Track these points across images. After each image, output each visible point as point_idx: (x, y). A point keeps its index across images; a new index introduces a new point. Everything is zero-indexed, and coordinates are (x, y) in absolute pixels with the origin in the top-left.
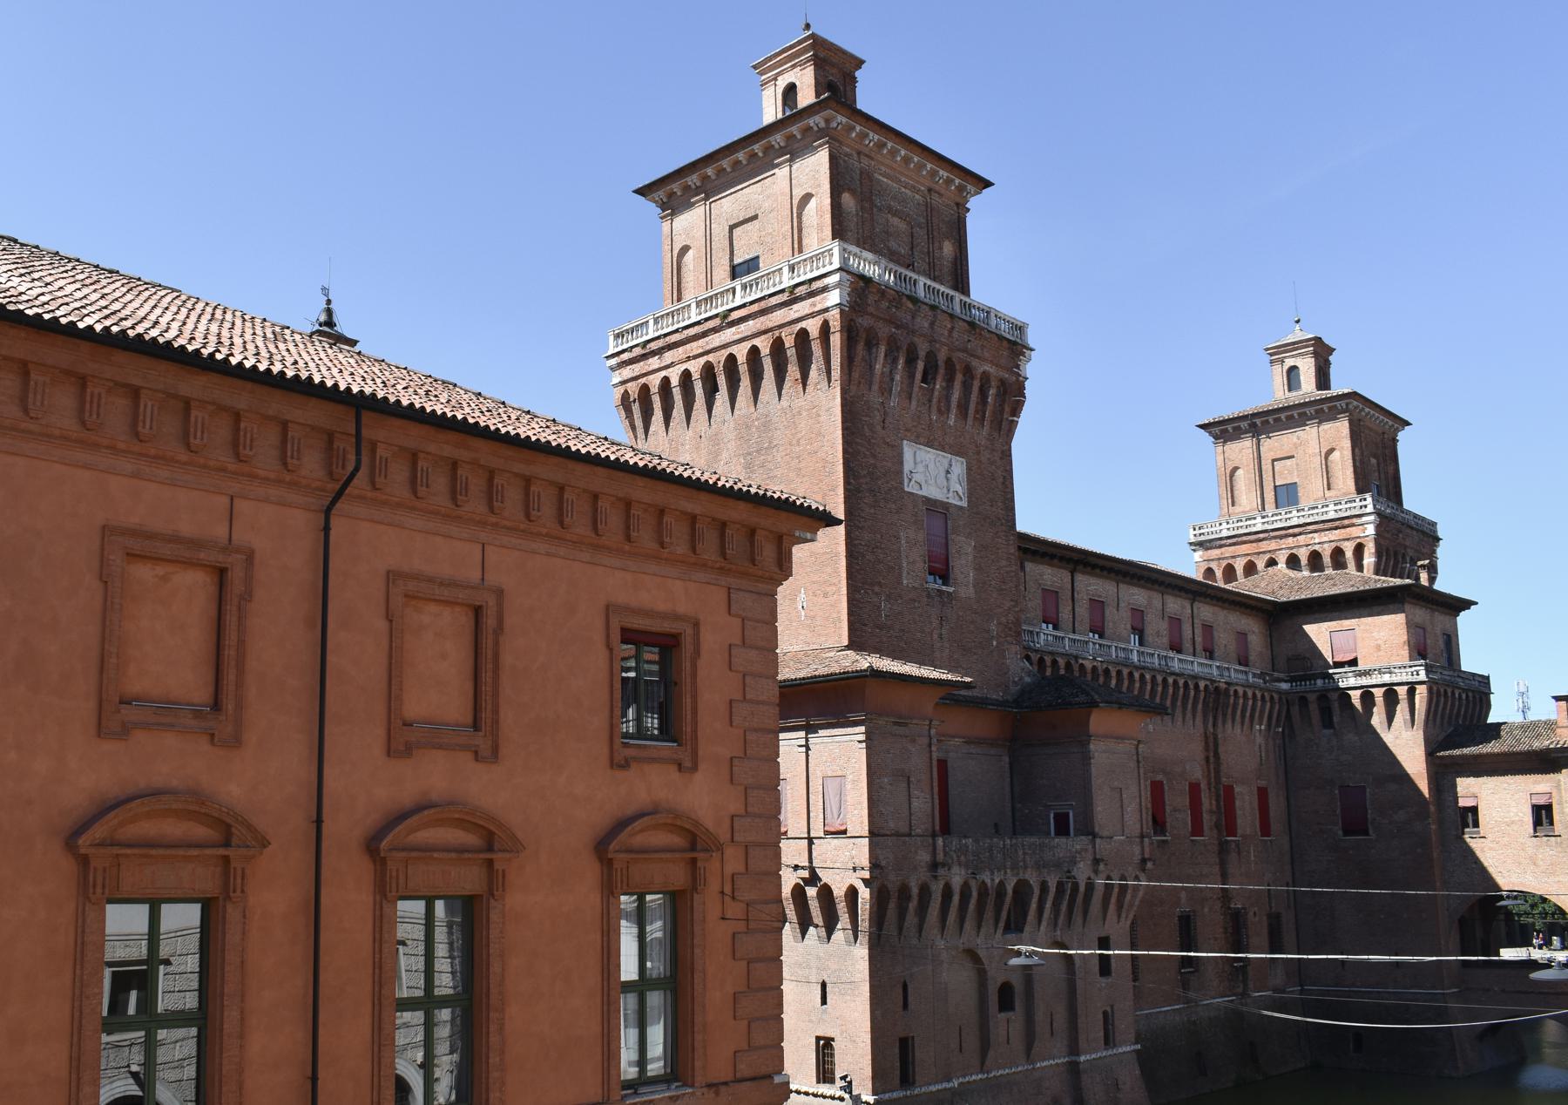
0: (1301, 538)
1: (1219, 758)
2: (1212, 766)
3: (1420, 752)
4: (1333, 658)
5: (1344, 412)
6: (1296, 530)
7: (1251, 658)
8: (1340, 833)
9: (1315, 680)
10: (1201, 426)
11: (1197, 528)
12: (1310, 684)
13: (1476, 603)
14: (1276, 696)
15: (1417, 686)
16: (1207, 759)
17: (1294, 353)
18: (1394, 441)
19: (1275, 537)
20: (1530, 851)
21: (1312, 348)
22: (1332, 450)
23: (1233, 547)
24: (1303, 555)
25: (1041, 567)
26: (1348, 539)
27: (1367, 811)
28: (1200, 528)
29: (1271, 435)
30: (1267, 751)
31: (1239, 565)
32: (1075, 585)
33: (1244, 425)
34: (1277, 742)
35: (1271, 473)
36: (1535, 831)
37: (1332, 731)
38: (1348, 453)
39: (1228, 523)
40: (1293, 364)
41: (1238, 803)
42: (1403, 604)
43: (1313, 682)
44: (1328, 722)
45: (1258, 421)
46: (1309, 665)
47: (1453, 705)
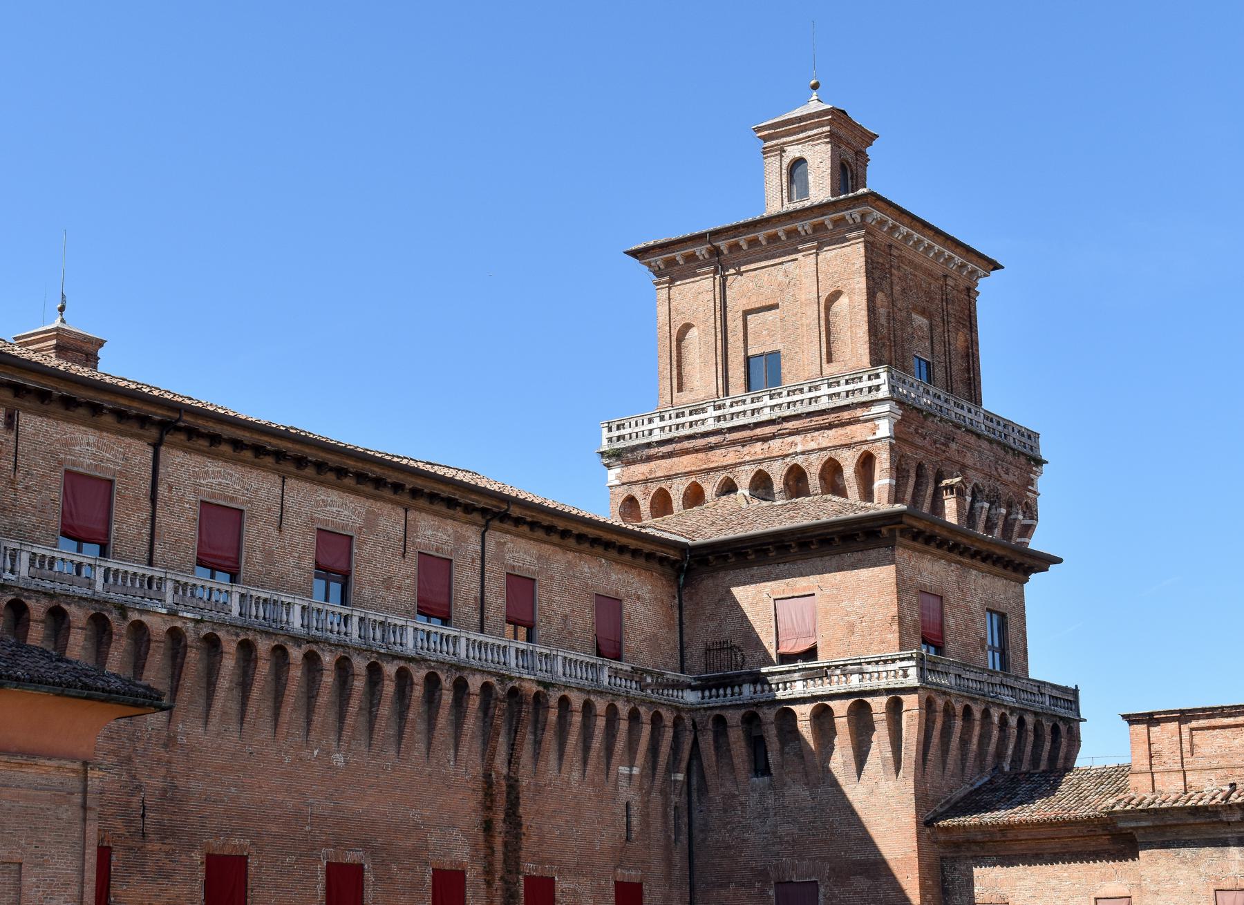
0: (776, 444)
1: (520, 825)
2: (498, 842)
3: (907, 819)
4: (778, 648)
5: (858, 228)
6: (767, 430)
7: (627, 644)
9: (740, 686)
10: (635, 254)
11: (614, 428)
12: (733, 695)
13: (1058, 561)
14: (668, 716)
15: (902, 697)
16: (488, 827)
17: (801, 136)
18: (970, 293)
19: (734, 443)
21: (828, 128)
22: (836, 295)
23: (668, 461)
24: (777, 472)
25: (69, 428)
26: (848, 446)
28: (618, 428)
29: (743, 268)
30: (645, 818)
31: (677, 491)
32: (162, 470)
33: (701, 251)
34: (674, 799)
35: (741, 335)
37: (766, 779)
38: (861, 300)
39: (662, 419)
40: (798, 155)
42: (893, 550)
43: (736, 689)
44: (761, 767)
45: (723, 245)
46: (739, 659)
47: (985, 737)
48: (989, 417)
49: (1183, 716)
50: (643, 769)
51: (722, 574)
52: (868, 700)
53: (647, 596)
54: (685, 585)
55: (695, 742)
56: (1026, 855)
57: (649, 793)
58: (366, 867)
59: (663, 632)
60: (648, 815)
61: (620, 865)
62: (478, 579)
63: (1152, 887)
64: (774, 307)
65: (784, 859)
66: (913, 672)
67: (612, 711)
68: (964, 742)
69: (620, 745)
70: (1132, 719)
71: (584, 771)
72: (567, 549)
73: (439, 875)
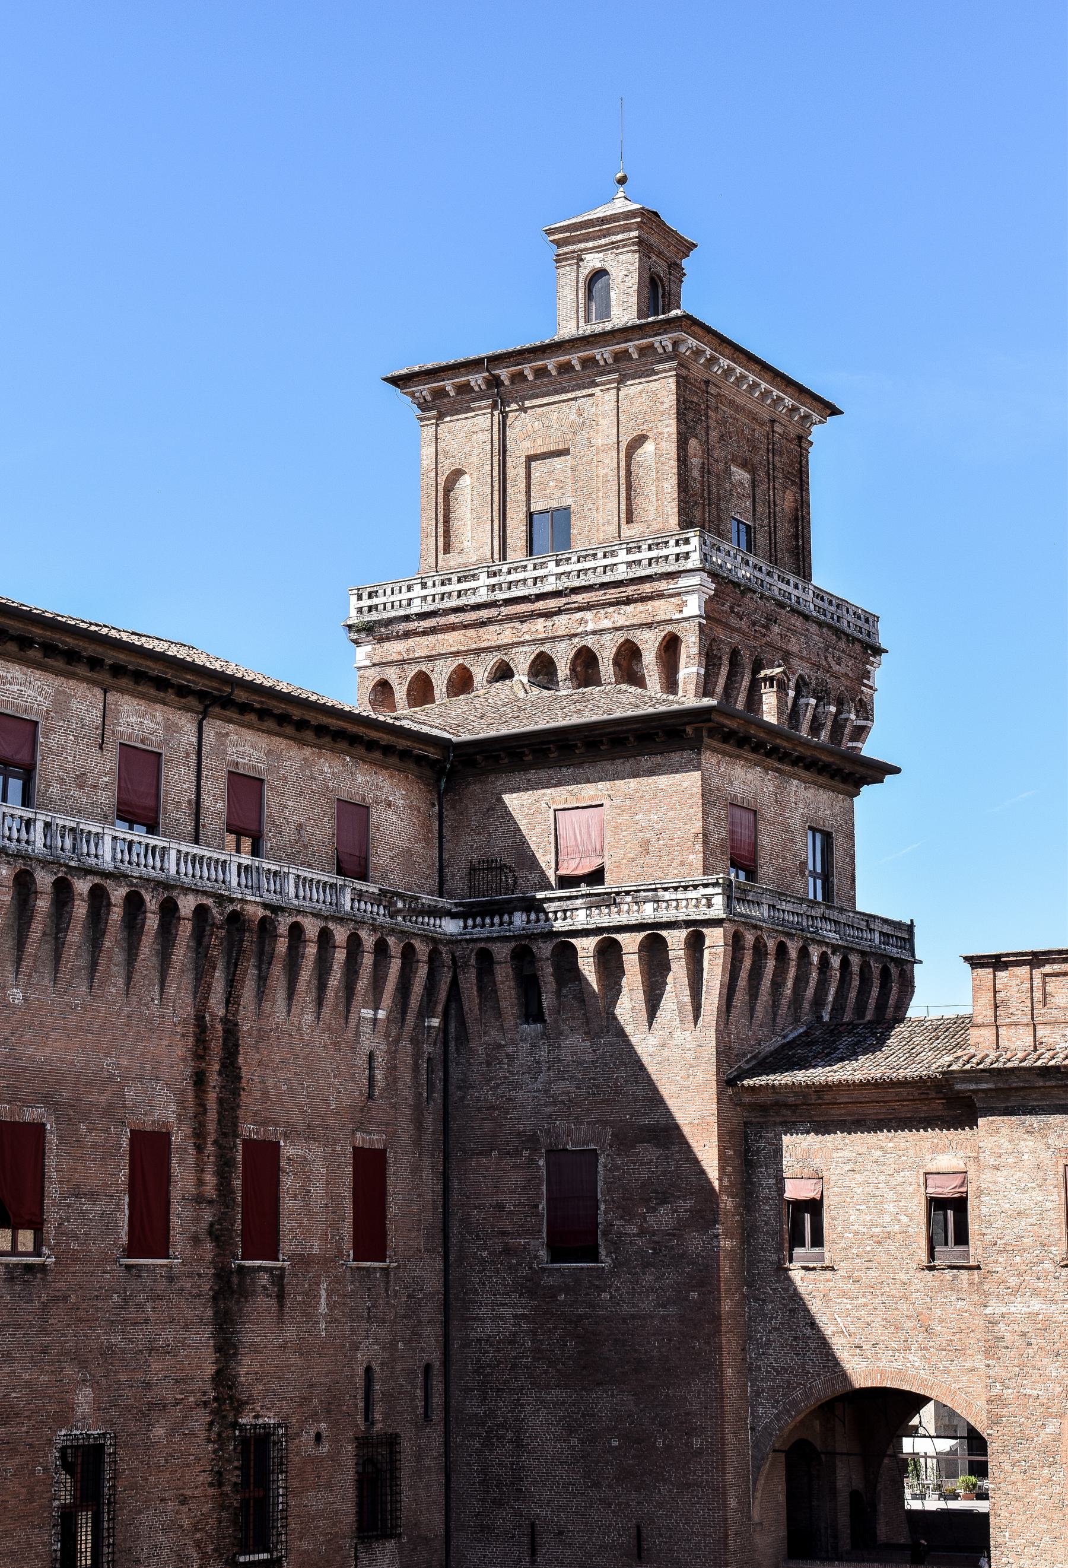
0: (562, 620)
1: (239, 1078)
2: (212, 1096)
3: (707, 1076)
4: (557, 869)
5: (670, 359)
6: (552, 604)
7: (373, 860)
8: (543, 1253)
9: (511, 914)
10: (396, 381)
11: (365, 596)
12: (501, 924)
13: (896, 770)
14: (422, 949)
15: (704, 930)
16: (199, 1080)
17: (603, 241)
18: (802, 442)
19: (511, 618)
20: (920, 1299)
21: (635, 233)
22: (640, 440)
23: (430, 638)
24: (563, 656)
26: (648, 626)
27: (598, 1208)
28: (370, 596)
29: (527, 404)
30: (392, 1069)
31: (440, 675)
33: (477, 380)
34: (427, 1049)
35: (523, 485)
36: (931, 1255)
38: (670, 447)
39: (424, 586)
40: (598, 265)
41: (287, 1182)
42: (699, 753)
43: (506, 918)
45: (504, 373)
46: (510, 881)
47: (801, 980)
48: (820, 594)
49: (1036, 959)
50: (390, 1012)
51: (491, 778)
52: (664, 933)
53: (400, 803)
54: (447, 790)
55: (454, 983)
56: (845, 1120)
57: (397, 1041)
58: (48, 1126)
59: (418, 847)
60: (395, 1067)
61: (360, 1127)
62: (193, 778)
63: (992, 1162)
64: (564, 452)
65: (558, 1123)
66: (718, 901)
67: (354, 943)
68: (777, 985)
69: (363, 982)
70: (975, 962)
71: (319, 1014)
72: (302, 743)
73: (138, 1138)
